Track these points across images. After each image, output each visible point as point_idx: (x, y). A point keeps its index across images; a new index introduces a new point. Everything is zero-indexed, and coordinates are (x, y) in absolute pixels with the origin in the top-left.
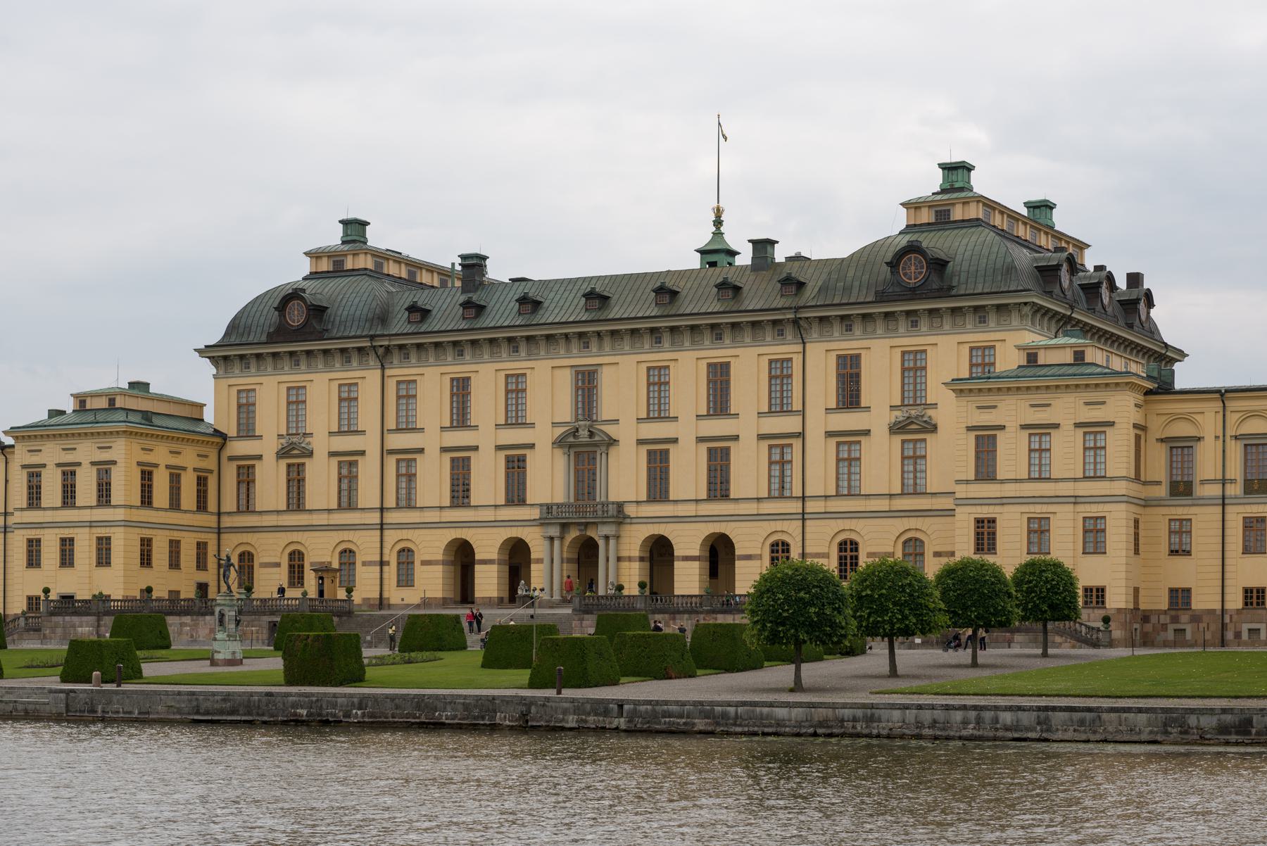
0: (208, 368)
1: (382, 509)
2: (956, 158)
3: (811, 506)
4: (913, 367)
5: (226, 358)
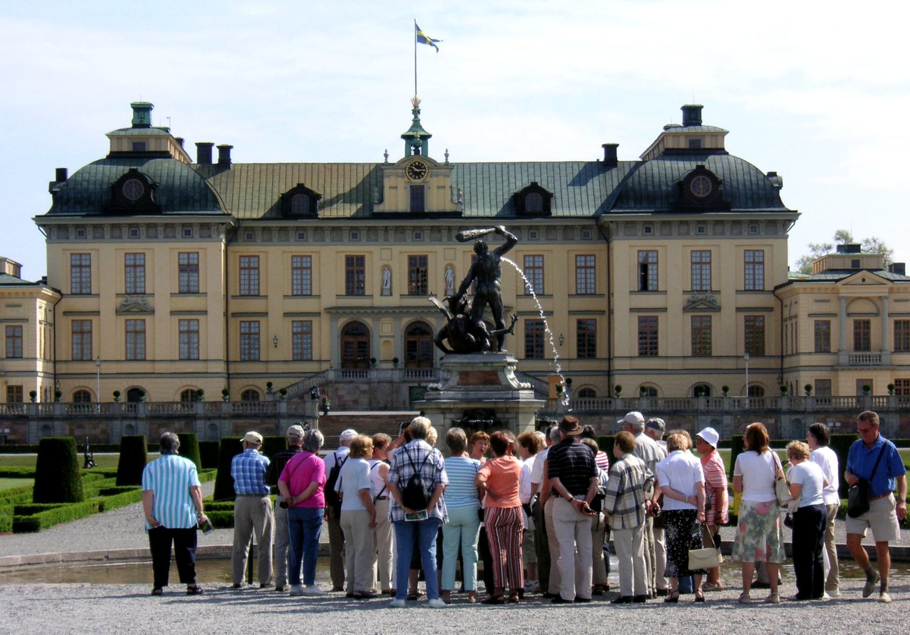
0: (39, 237)
1: (228, 362)
2: (690, 102)
3: (617, 364)
4: (701, 263)
5: (59, 227)
